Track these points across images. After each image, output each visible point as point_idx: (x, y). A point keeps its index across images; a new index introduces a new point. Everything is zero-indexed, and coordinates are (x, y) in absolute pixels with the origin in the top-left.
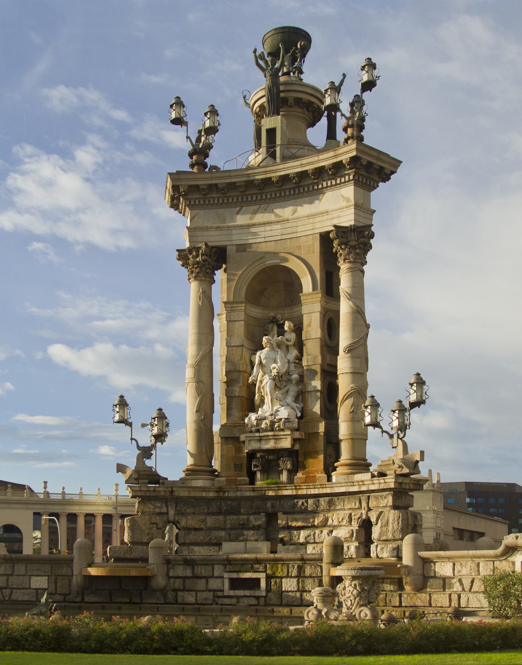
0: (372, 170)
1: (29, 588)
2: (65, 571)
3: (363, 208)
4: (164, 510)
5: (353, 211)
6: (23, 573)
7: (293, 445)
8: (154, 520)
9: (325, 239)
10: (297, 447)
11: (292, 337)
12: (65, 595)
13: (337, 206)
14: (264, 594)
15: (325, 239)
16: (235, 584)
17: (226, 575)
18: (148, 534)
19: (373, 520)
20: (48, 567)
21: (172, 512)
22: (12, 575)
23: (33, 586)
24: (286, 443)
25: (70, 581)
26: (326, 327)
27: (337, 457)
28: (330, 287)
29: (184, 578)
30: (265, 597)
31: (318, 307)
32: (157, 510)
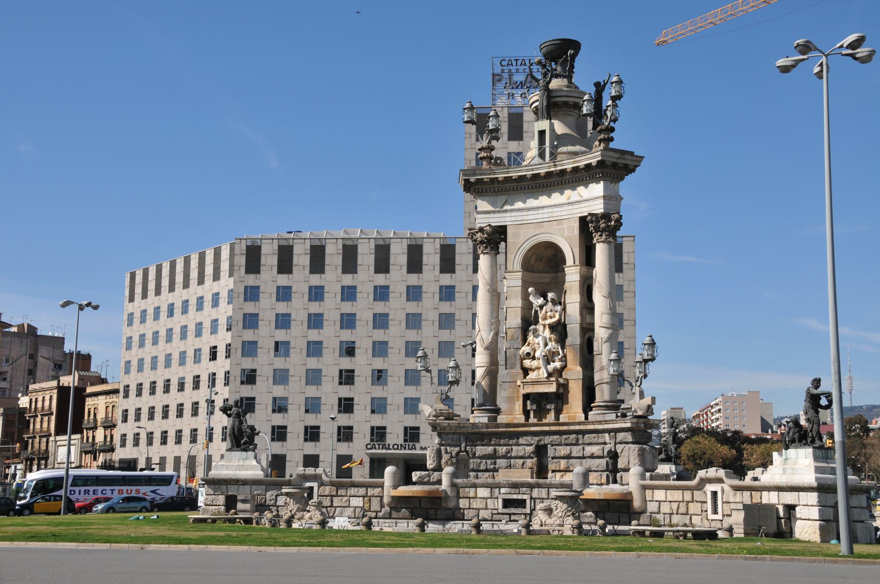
0: (615, 168)
2: (377, 491)
3: (611, 198)
5: (602, 201)
7: (558, 389)
9: (583, 221)
10: (561, 391)
12: (377, 512)
13: (591, 197)
14: (529, 512)
15: (583, 221)
16: (507, 503)
19: (619, 451)
24: (552, 388)
28: (588, 259)
31: (577, 277)
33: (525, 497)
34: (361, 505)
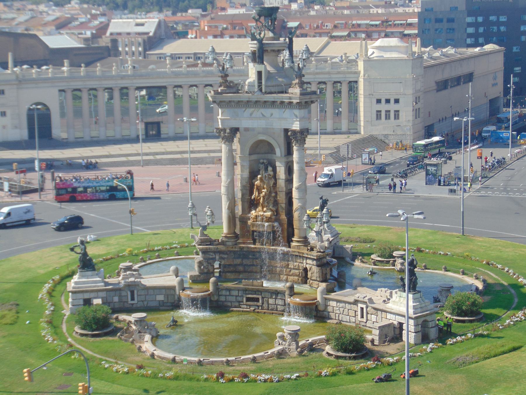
1: (156, 300)
4: (214, 256)
6: (152, 293)
8: (209, 262)
11: (272, 173)
16: (248, 299)
17: (244, 295)
18: (207, 268)
19: (308, 269)
20: (164, 291)
21: (217, 257)
22: (148, 295)
23: (157, 299)
25: (174, 296)
26: (287, 172)
27: (293, 235)
29: (226, 296)
30: (262, 306)
32: (211, 257)
33: (258, 296)
34: (163, 299)
